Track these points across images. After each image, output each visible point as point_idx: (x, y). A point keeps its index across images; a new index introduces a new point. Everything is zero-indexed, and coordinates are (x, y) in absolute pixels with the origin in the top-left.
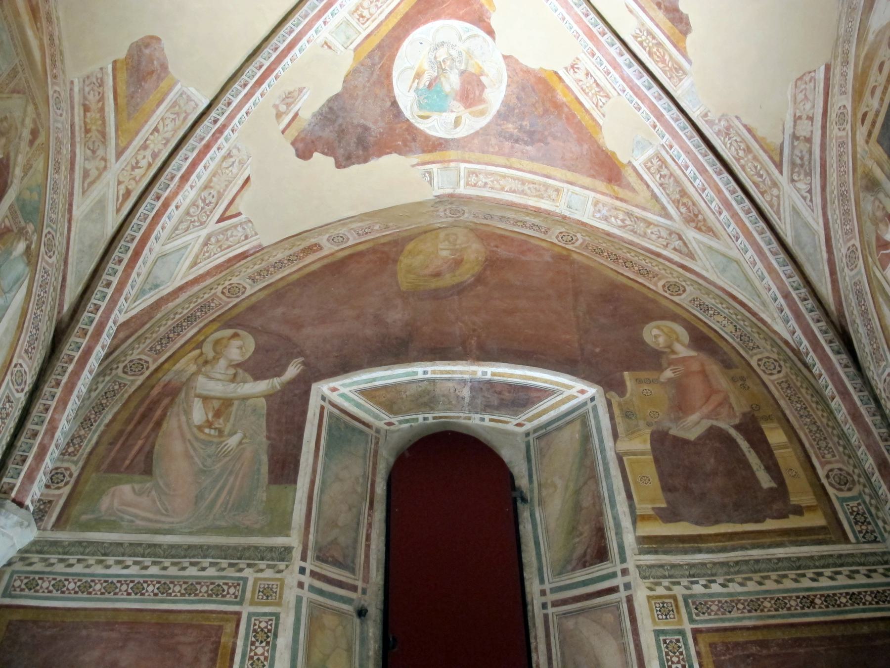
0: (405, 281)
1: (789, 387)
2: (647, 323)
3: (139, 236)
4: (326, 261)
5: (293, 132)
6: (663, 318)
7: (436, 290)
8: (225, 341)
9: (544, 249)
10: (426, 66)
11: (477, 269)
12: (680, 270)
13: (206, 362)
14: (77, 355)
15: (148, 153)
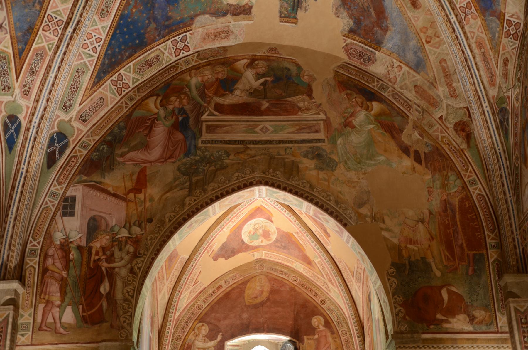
0: (247, 302)
1: (347, 341)
2: (313, 317)
3: (176, 304)
4: (224, 293)
5: (213, 255)
6: (318, 315)
7: (256, 304)
8: (200, 327)
9: (287, 285)
10: (252, 230)
11: (268, 294)
12: (326, 294)
13: (197, 336)
14: (167, 343)
15: (174, 276)
